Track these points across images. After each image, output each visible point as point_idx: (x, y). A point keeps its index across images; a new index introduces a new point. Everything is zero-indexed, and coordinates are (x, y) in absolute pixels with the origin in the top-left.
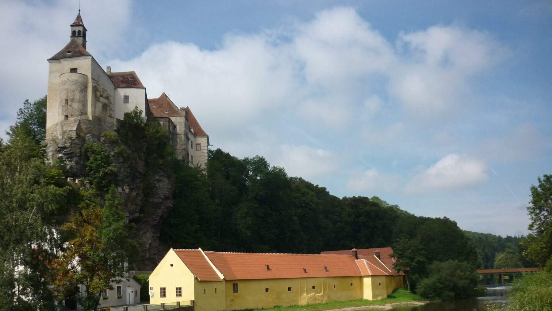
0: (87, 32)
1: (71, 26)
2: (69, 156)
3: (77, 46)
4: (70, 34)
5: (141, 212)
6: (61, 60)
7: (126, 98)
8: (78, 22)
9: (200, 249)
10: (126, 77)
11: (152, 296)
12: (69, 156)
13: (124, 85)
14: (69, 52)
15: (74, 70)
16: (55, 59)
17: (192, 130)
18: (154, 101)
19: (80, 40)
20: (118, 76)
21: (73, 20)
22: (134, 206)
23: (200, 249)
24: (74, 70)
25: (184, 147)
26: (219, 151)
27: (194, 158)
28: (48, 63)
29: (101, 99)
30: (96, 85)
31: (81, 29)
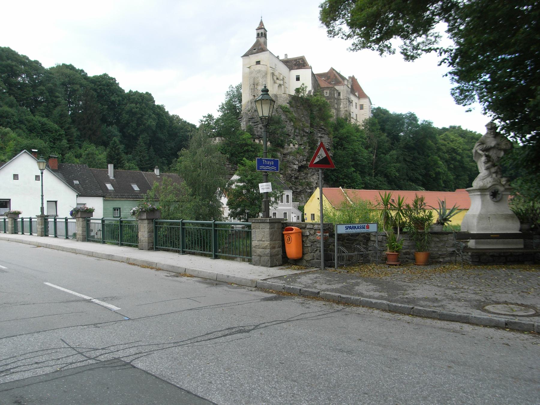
0: (267, 33)
1: (257, 30)
2: (256, 124)
3: (260, 45)
4: (256, 36)
5: (307, 160)
6: (250, 56)
7: (298, 79)
8: (261, 27)
9: (340, 187)
10: (298, 60)
11: (306, 219)
12: (256, 124)
13: (296, 68)
14: (255, 50)
15: (258, 63)
16: (246, 55)
17: (357, 94)
18: (321, 75)
19: (262, 40)
20: (292, 60)
21: (257, 25)
22: (301, 157)
23: (340, 187)
24: (258, 63)
25: (346, 109)
26: (379, 109)
27: (358, 116)
28: (241, 58)
29: (278, 82)
30: (273, 71)
31: (262, 31)
